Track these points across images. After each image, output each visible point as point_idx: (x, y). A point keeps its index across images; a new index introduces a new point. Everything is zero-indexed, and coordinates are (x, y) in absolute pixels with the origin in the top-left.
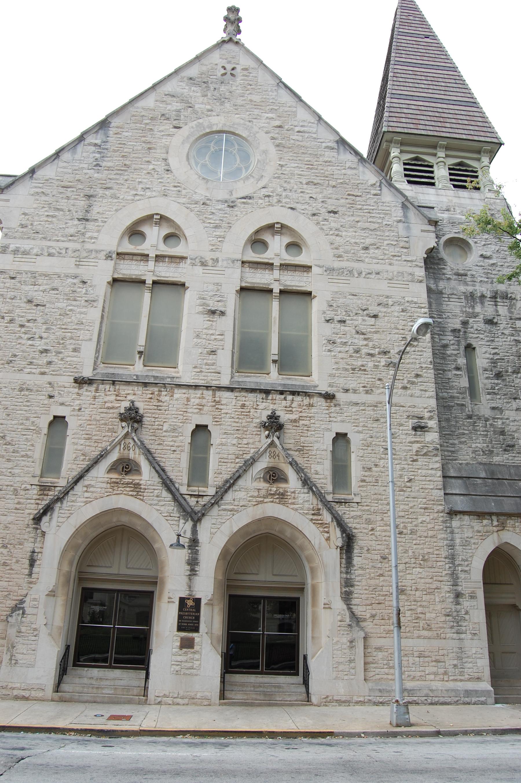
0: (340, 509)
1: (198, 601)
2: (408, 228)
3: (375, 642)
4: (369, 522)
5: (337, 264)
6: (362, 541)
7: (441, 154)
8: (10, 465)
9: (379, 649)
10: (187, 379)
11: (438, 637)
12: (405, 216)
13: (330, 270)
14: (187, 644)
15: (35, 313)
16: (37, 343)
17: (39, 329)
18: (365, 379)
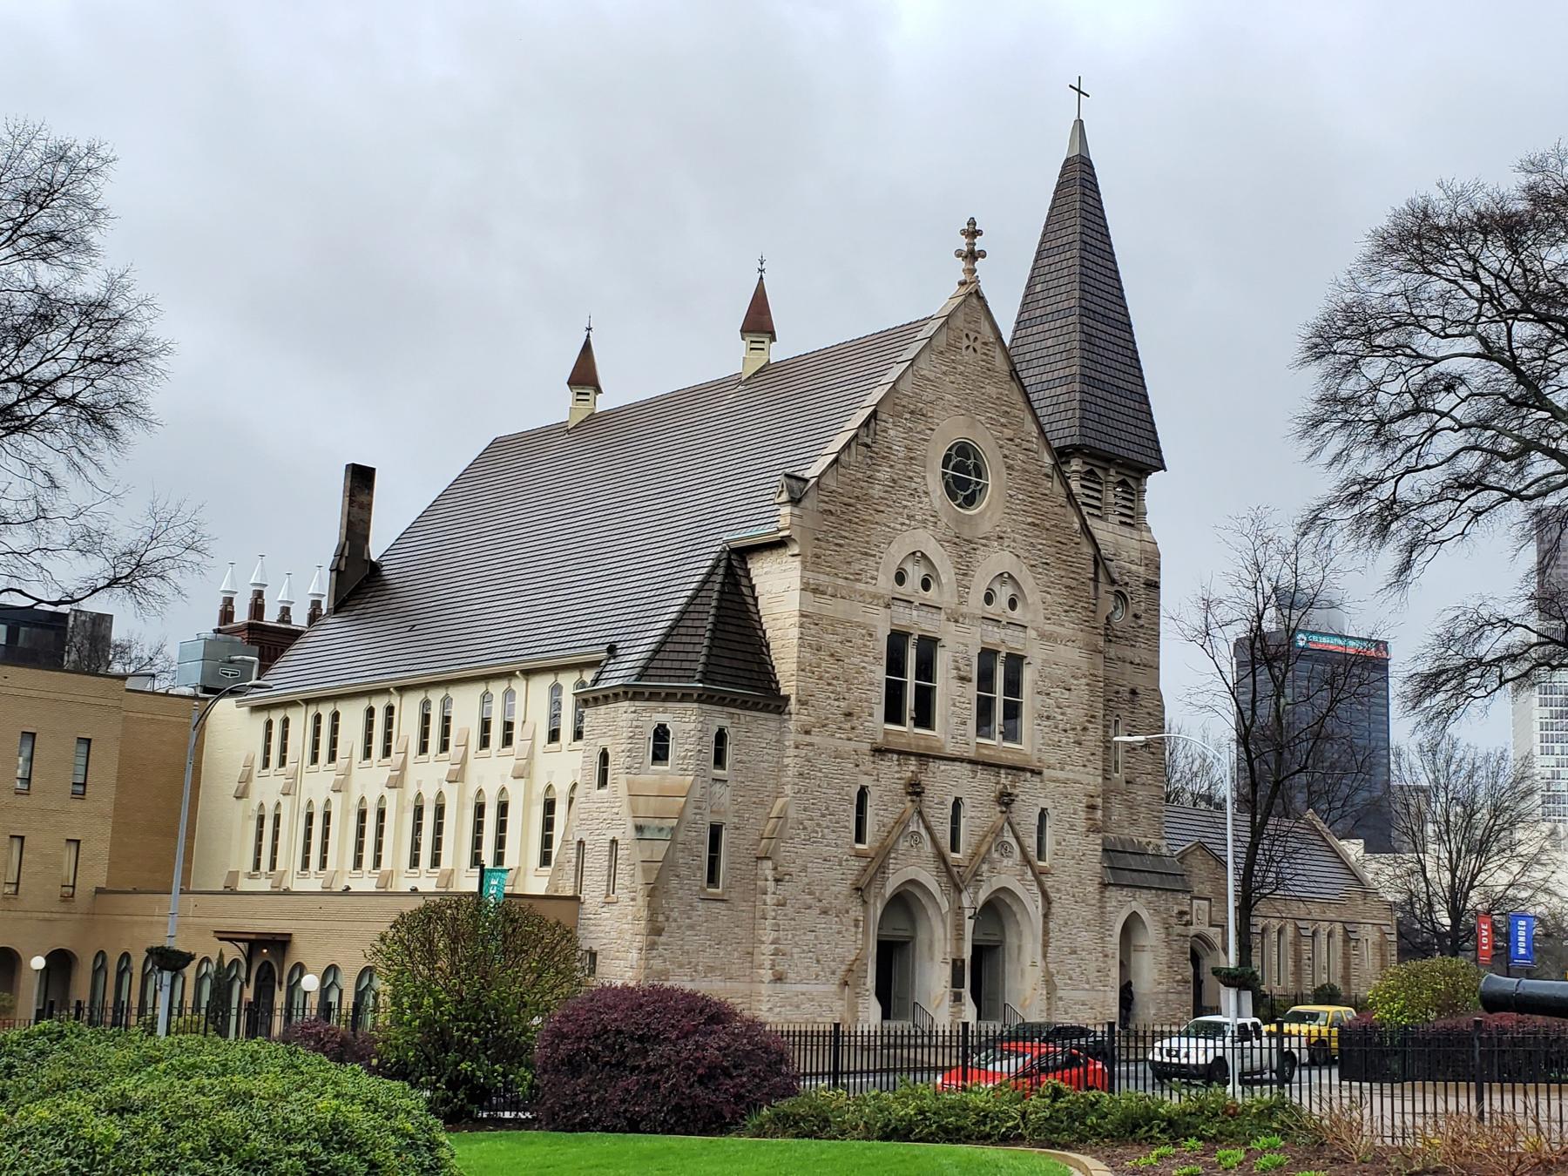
0: (1043, 878)
1: (963, 961)
2: (1096, 588)
3: (1060, 993)
4: (1058, 890)
5: (1049, 628)
6: (1056, 908)
7: (1112, 472)
8: (834, 836)
9: (1061, 999)
10: (950, 749)
11: (1093, 989)
12: (1096, 573)
13: (1042, 636)
14: (957, 998)
15: (835, 669)
16: (842, 704)
17: (840, 687)
18: (1060, 755)
